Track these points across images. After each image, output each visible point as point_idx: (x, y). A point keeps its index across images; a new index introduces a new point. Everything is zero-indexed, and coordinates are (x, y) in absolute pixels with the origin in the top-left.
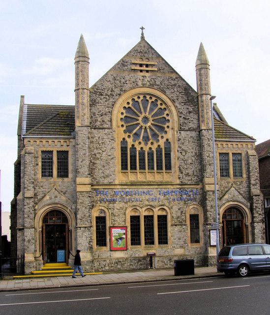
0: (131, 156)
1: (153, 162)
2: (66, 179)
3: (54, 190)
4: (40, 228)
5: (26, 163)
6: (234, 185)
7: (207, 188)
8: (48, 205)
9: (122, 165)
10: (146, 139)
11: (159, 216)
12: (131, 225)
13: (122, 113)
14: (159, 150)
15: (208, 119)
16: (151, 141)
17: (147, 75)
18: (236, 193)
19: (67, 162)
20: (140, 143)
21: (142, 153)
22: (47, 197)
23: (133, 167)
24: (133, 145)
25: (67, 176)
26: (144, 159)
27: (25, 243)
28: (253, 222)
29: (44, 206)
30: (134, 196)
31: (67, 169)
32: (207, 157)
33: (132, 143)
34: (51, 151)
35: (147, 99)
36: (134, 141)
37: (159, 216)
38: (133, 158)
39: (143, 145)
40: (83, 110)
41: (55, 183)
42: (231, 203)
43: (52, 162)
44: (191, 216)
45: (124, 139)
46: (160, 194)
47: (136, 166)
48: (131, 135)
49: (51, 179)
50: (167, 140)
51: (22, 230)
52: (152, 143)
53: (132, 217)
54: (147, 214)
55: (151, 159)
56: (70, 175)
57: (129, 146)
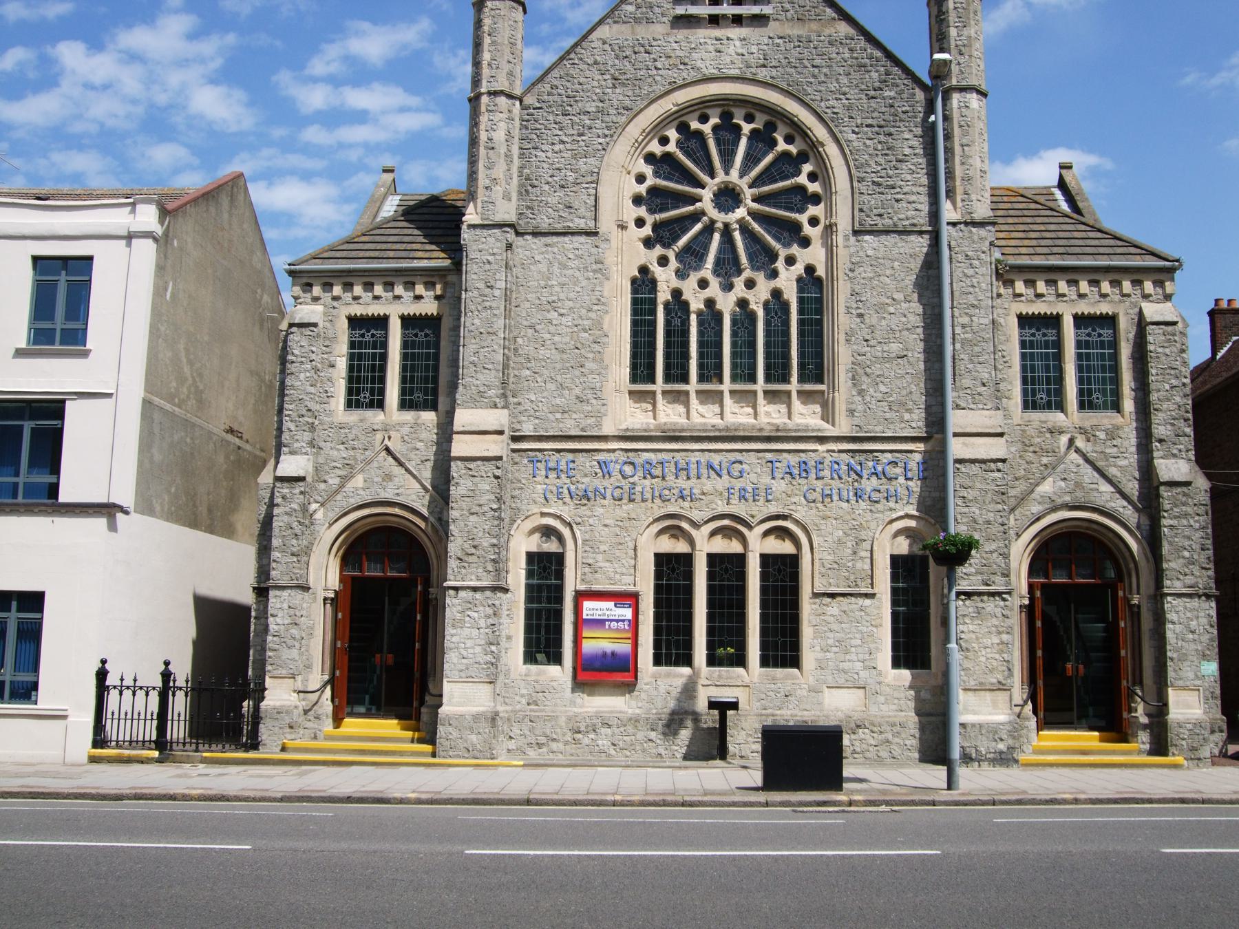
1: (753, 355)
9: (634, 367)
10: (728, 267)
12: (658, 589)
13: (641, 179)
16: (747, 273)
17: (735, 32)
20: (703, 284)
21: (711, 315)
22: (358, 481)
23: (676, 372)
24: (677, 293)
33: (675, 283)
36: (681, 275)
38: (677, 338)
39: (714, 289)
43: (384, 357)
45: (644, 270)
48: (671, 255)
50: (810, 269)
52: (750, 284)
53: (662, 560)
57: (663, 295)
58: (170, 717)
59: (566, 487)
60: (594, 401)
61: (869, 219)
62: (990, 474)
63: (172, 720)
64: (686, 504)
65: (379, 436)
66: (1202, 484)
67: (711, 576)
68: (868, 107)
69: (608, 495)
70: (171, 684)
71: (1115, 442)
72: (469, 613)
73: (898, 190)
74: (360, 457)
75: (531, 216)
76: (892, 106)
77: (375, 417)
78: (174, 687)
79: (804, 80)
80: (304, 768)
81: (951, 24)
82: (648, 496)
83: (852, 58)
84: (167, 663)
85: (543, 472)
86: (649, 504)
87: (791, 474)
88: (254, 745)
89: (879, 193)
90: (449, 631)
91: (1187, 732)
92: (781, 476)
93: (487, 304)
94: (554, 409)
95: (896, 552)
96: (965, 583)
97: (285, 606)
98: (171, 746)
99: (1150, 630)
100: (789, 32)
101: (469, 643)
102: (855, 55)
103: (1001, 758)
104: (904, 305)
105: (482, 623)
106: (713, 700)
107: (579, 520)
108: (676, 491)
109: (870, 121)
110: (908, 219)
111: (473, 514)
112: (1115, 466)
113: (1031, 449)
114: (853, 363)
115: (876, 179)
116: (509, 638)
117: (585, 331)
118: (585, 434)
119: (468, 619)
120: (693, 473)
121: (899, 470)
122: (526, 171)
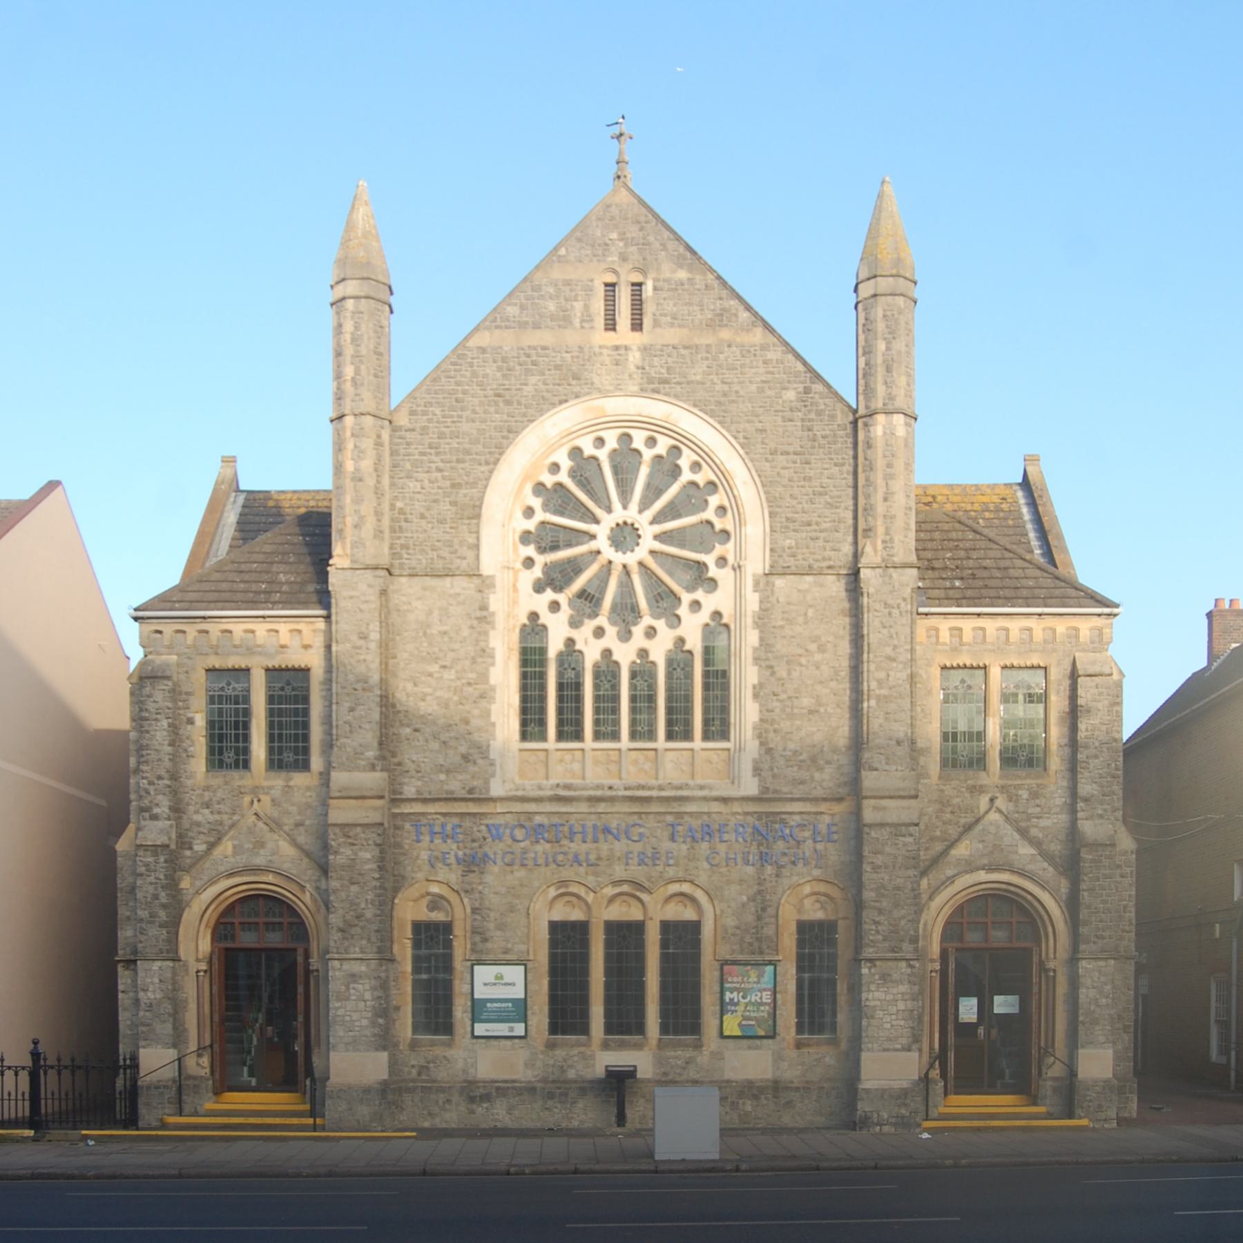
0: (560, 687)
2: (299, 779)
4: (198, 960)
5: (146, 714)
6: (1000, 803)
7: (869, 815)
8: (231, 875)
9: (524, 723)
10: (626, 614)
11: (666, 926)
13: (529, 512)
14: (679, 661)
15: (889, 517)
16: (647, 620)
18: (1010, 835)
19: (306, 712)
20: (599, 632)
22: (227, 847)
23: (570, 729)
24: (570, 642)
25: (305, 766)
26: (616, 698)
27: (141, 1014)
28: (1073, 960)
29: (212, 882)
30: (565, 842)
31: (306, 738)
32: (879, 682)
34: (240, 670)
35: (635, 445)
36: (575, 623)
37: (666, 926)
39: (611, 639)
40: (358, 500)
41: (256, 790)
42: (982, 876)
43: (247, 713)
44: (805, 929)
45: (534, 616)
46: (672, 838)
47: (579, 723)
49: (242, 778)
50: (717, 615)
51: (131, 963)
53: (556, 928)
54: (616, 912)
55: (643, 700)
56: (316, 762)
58: (43, 1096)
59: (452, 853)
60: (480, 762)
61: (781, 561)
62: (901, 838)
63: (46, 1099)
64: (582, 870)
65: (247, 799)
66: (1126, 842)
67: (608, 944)
70: (42, 1062)
71: (1038, 801)
72: (356, 986)
73: (815, 527)
74: (227, 822)
75: (406, 556)
76: (810, 430)
77: (237, 778)
78: (45, 1066)
79: (712, 399)
80: (189, 1144)
81: (879, 335)
82: (540, 861)
84: (36, 1043)
85: (427, 838)
86: (543, 869)
87: (693, 838)
88: (132, 1121)
89: (794, 531)
90: (334, 1004)
91: (1094, 1095)
92: (682, 840)
93: (362, 657)
94: (440, 768)
95: (805, 917)
96: (871, 950)
97: (156, 980)
98: (47, 1125)
99: (1065, 994)
100: (696, 341)
101: (355, 1016)
102: (771, 369)
104: (818, 657)
105: (368, 996)
106: (610, 1069)
107: (468, 887)
108: (571, 857)
109: (786, 448)
110: (824, 559)
111: (354, 884)
112: (1036, 826)
113: (949, 809)
114: (761, 720)
116: (397, 1008)
117: (469, 684)
118: (471, 796)
120: (590, 837)
121: (807, 834)
122: (399, 504)
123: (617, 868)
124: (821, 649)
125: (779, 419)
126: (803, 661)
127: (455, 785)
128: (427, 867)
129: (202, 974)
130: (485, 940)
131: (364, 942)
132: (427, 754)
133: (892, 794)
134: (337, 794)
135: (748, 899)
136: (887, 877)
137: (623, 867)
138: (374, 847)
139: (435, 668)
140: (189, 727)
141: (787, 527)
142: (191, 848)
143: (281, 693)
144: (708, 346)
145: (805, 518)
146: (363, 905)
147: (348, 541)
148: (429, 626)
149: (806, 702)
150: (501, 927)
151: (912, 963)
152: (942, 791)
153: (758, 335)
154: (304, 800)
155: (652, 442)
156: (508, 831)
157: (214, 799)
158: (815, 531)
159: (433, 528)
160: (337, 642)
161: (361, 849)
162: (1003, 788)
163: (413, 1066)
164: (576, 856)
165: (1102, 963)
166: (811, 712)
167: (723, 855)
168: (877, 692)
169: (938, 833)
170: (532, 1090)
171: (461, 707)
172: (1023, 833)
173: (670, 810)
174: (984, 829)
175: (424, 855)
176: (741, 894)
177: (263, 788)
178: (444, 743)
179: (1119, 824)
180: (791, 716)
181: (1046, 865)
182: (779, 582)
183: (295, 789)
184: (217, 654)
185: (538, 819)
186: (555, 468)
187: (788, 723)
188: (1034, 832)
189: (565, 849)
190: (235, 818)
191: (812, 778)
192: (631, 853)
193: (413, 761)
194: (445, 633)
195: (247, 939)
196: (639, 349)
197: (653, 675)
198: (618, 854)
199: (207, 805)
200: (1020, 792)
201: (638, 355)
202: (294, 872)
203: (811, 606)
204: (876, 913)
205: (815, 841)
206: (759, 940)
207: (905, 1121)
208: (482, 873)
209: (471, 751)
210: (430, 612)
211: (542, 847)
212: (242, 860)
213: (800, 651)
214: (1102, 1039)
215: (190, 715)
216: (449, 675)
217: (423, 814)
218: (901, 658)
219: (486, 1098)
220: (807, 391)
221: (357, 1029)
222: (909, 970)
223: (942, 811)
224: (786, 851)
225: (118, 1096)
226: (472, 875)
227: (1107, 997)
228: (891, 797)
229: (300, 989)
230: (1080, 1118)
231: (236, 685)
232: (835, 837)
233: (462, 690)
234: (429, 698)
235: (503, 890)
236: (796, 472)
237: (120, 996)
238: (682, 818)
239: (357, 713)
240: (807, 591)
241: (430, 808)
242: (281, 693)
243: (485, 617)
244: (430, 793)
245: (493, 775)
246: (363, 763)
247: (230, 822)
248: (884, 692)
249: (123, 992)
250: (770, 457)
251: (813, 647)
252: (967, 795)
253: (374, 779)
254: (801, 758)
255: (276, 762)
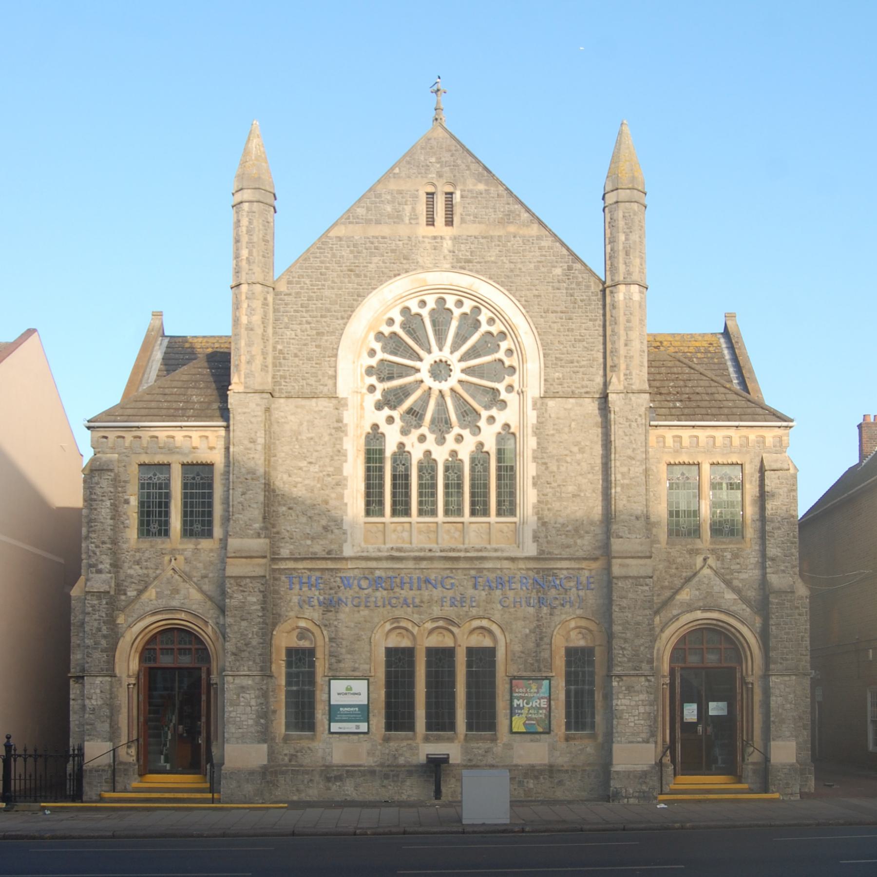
0: (394, 477)
2: (205, 544)
3: (171, 572)
4: (129, 676)
5: (94, 497)
6: (711, 561)
7: (616, 570)
8: (154, 613)
9: (368, 504)
10: (441, 425)
13: (372, 353)
14: (479, 459)
16: (456, 430)
18: (718, 586)
19: (211, 496)
20: (422, 438)
22: (151, 593)
23: (401, 507)
24: (401, 445)
25: (209, 534)
26: (434, 486)
27: (87, 716)
28: (766, 676)
29: (141, 618)
30: (397, 590)
31: (210, 514)
32: (623, 474)
35: (447, 306)
36: (405, 432)
37: (470, 651)
40: (250, 344)
41: (173, 552)
42: (699, 614)
43: (168, 496)
45: (375, 427)
46: (475, 587)
47: (408, 504)
49: (163, 543)
50: (507, 426)
51: (80, 678)
54: (435, 641)
55: (454, 487)
56: (218, 531)
58: (13, 777)
59: (316, 597)
61: (552, 388)
62: (640, 587)
63: (15, 780)
64: (409, 610)
65: (167, 558)
66: (802, 590)
67: (429, 664)
68: (554, 296)
69: (349, 604)
70: (13, 752)
71: (738, 561)
72: (243, 695)
73: (576, 364)
76: (572, 296)
77: (160, 543)
78: (15, 755)
79: (503, 274)
81: (620, 230)
82: (380, 603)
83: (541, 255)
84: (8, 738)
85: (297, 587)
86: (381, 610)
87: (490, 586)
88: (78, 796)
89: (561, 366)
90: (228, 709)
92: (482, 588)
93: (251, 456)
94: (307, 536)
95: (571, 645)
96: (619, 669)
97: (98, 691)
98: (15, 799)
99: (760, 701)
100: (491, 233)
101: (244, 717)
102: (544, 253)
103: (644, 796)
104: (579, 456)
105: (253, 703)
107: (327, 623)
108: (401, 600)
109: (555, 308)
110: (583, 387)
111: (244, 620)
112: (737, 579)
113: (674, 566)
114: (539, 501)
115: (557, 356)
116: (274, 712)
117: (329, 475)
118: (330, 556)
119: (242, 699)
121: (572, 584)
122: (279, 347)
123: (435, 608)
124: (582, 451)
125: (550, 288)
126: (568, 459)
127: (318, 548)
128: (297, 608)
129: (132, 686)
130: (339, 661)
131: (251, 663)
132: (298, 525)
133: (633, 555)
134: (233, 555)
135: (530, 631)
136: (630, 615)
137: (439, 608)
138: (258, 593)
139: (303, 464)
140: (126, 506)
141: (556, 364)
142: (125, 594)
143: (192, 481)
144: (500, 237)
145: (569, 358)
146: (250, 636)
147: (242, 373)
148: (300, 434)
149: (571, 488)
150: (351, 651)
151: (649, 678)
152: (669, 553)
153: (535, 230)
154: (208, 559)
155: (460, 304)
156: (356, 582)
157: (143, 558)
158: (576, 367)
159: (303, 364)
160: (234, 445)
161: (249, 595)
162: (713, 551)
163: (286, 755)
164: (405, 600)
165: (787, 678)
166: (574, 496)
167: (512, 599)
168: (622, 481)
169: (666, 583)
170: (372, 772)
171: (322, 492)
172: (728, 583)
173: (473, 566)
174: (699, 581)
175: (295, 599)
176: (524, 628)
177: (178, 550)
178: (310, 517)
179: (797, 577)
180: (560, 499)
181: (744, 606)
182: (551, 403)
183: (202, 551)
184: (146, 453)
185: (378, 573)
186: (391, 322)
187: (558, 504)
188: (736, 583)
189: (397, 595)
190: (158, 572)
191: (575, 543)
192: (445, 597)
193: (288, 531)
194: (312, 439)
195: (166, 661)
196: (451, 239)
197: (460, 469)
198: (436, 599)
199: (138, 563)
200: (725, 554)
201: (450, 243)
202: (200, 611)
203: (573, 420)
204: (622, 641)
205: (578, 589)
206: (538, 661)
207: (646, 794)
208: (337, 612)
209: (329, 524)
210: (301, 424)
211: (381, 594)
212: (162, 603)
213: (567, 452)
214: (787, 734)
215: (126, 497)
216: (314, 469)
217: (294, 569)
218: (638, 458)
219: (339, 778)
220: (570, 268)
221: (245, 727)
222: (647, 684)
223: (669, 568)
224: (557, 596)
225: (68, 777)
226: (330, 614)
227: (791, 703)
228: (632, 557)
229: (204, 697)
230: (773, 792)
231: (160, 476)
232: (592, 586)
233: (323, 480)
234: (299, 485)
235: (352, 625)
236: (562, 326)
237: (72, 702)
238: (482, 572)
239: (247, 496)
240: (570, 409)
241: (300, 565)
242: (192, 481)
243: (341, 427)
244: (300, 554)
245: (346, 541)
246: (252, 532)
247: (154, 575)
248: (626, 481)
249: (73, 700)
250: (544, 315)
251: (575, 449)
252: (687, 556)
253: (258, 544)
254: (568, 529)
255: (188, 532)
